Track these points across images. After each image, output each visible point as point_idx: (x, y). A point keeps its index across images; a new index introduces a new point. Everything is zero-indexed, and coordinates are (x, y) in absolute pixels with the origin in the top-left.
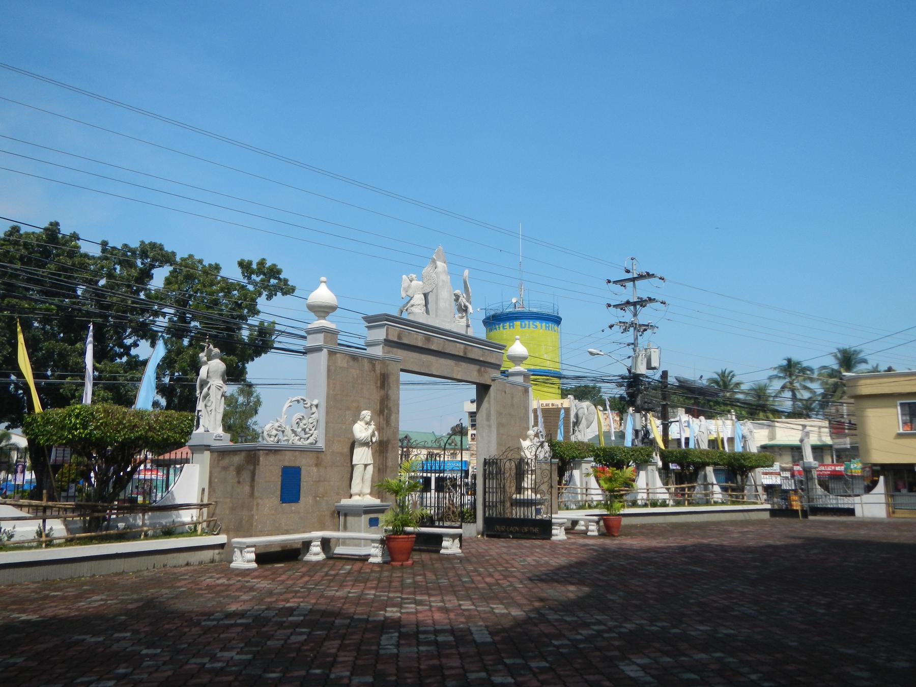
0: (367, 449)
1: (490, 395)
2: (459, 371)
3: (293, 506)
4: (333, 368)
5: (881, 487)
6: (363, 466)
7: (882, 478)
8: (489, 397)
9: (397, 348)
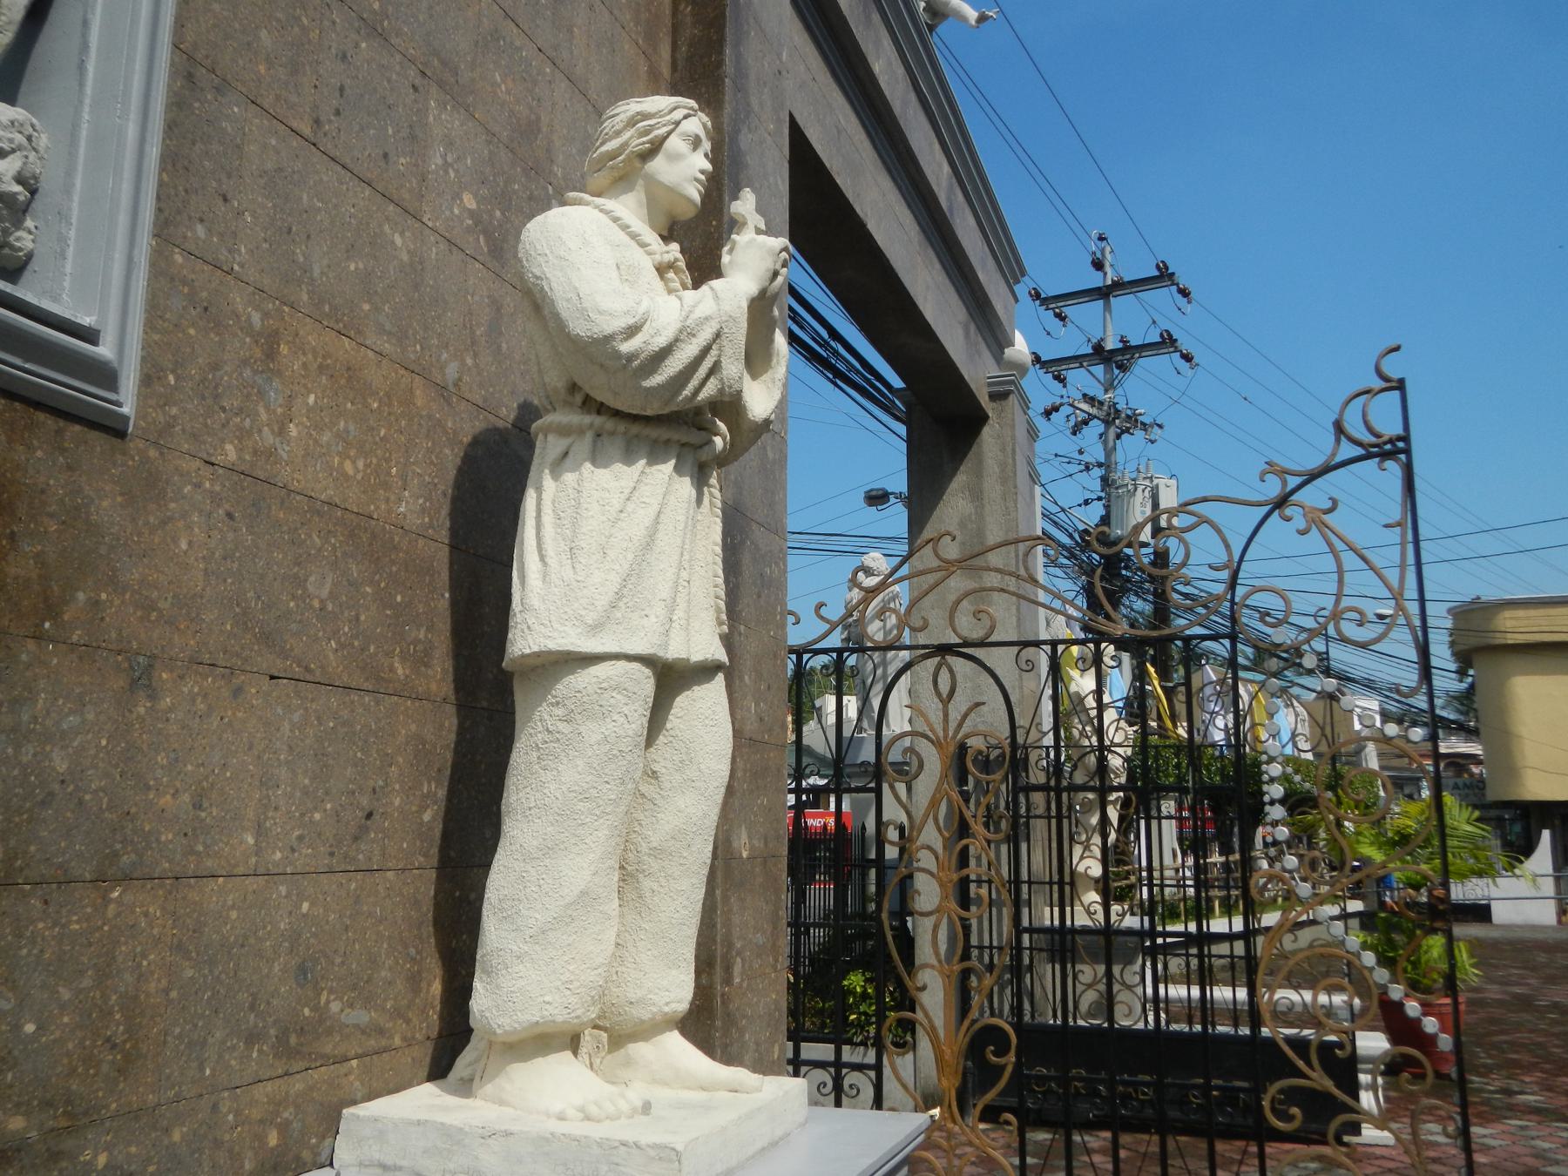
0: (685, 487)
1: (980, 461)
5: (1543, 857)
6: (645, 682)
7: (1546, 835)
8: (979, 474)
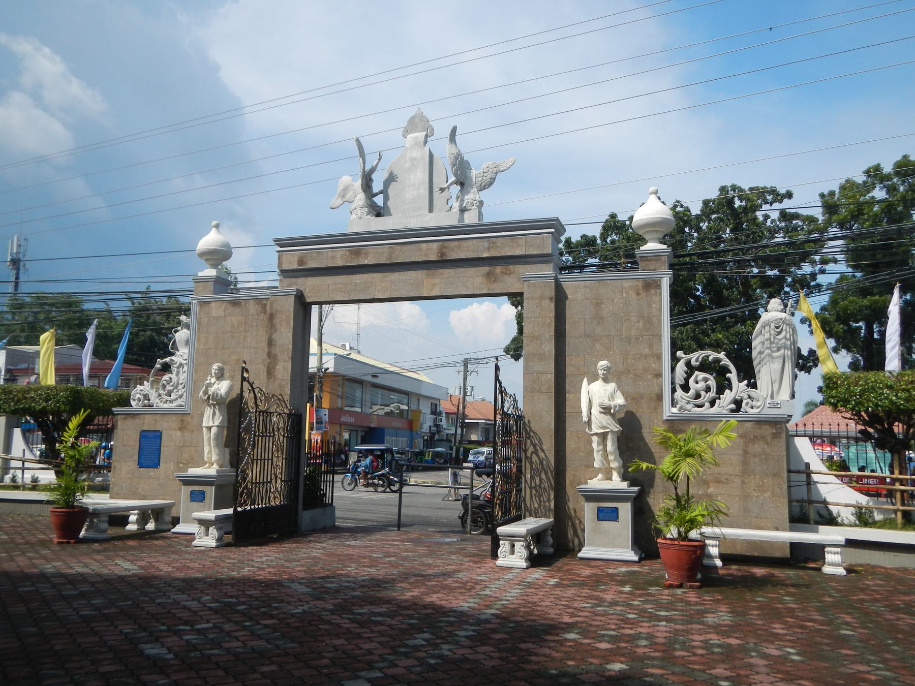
2: (435, 284)
3: (152, 472)
4: (205, 320)
9: (306, 276)
